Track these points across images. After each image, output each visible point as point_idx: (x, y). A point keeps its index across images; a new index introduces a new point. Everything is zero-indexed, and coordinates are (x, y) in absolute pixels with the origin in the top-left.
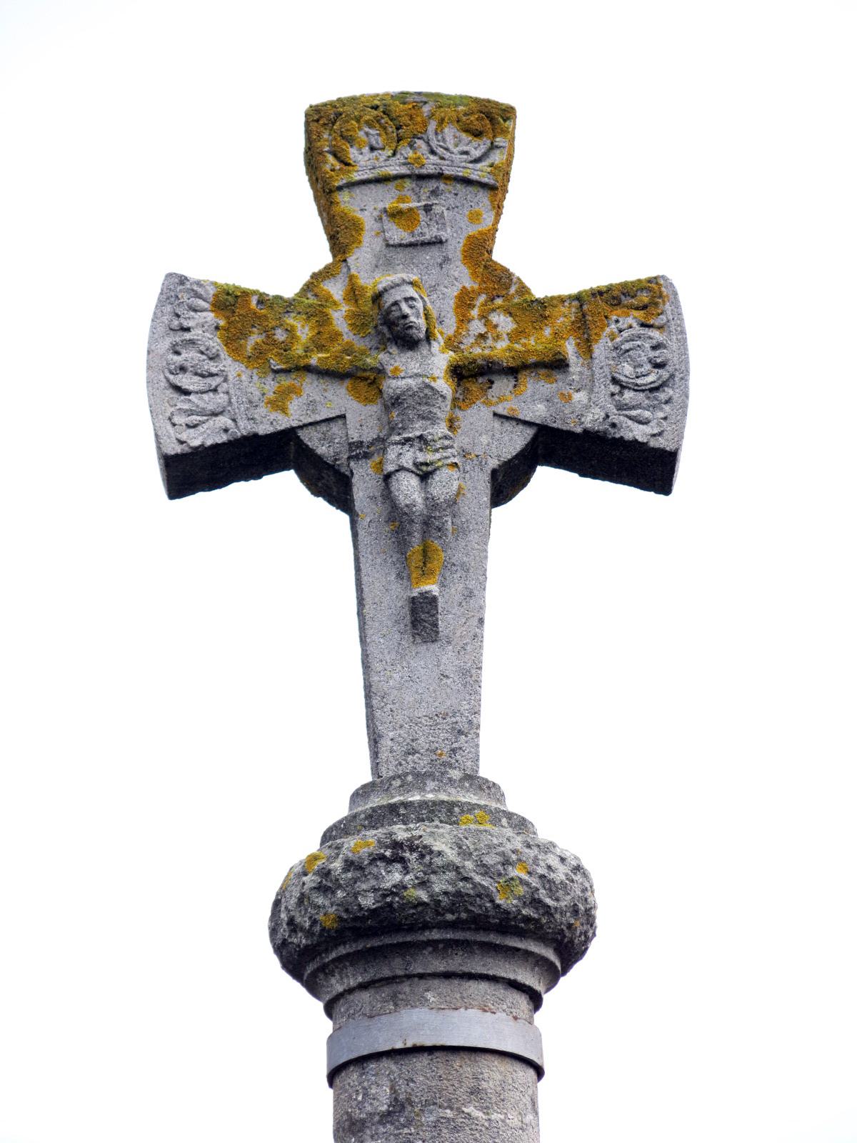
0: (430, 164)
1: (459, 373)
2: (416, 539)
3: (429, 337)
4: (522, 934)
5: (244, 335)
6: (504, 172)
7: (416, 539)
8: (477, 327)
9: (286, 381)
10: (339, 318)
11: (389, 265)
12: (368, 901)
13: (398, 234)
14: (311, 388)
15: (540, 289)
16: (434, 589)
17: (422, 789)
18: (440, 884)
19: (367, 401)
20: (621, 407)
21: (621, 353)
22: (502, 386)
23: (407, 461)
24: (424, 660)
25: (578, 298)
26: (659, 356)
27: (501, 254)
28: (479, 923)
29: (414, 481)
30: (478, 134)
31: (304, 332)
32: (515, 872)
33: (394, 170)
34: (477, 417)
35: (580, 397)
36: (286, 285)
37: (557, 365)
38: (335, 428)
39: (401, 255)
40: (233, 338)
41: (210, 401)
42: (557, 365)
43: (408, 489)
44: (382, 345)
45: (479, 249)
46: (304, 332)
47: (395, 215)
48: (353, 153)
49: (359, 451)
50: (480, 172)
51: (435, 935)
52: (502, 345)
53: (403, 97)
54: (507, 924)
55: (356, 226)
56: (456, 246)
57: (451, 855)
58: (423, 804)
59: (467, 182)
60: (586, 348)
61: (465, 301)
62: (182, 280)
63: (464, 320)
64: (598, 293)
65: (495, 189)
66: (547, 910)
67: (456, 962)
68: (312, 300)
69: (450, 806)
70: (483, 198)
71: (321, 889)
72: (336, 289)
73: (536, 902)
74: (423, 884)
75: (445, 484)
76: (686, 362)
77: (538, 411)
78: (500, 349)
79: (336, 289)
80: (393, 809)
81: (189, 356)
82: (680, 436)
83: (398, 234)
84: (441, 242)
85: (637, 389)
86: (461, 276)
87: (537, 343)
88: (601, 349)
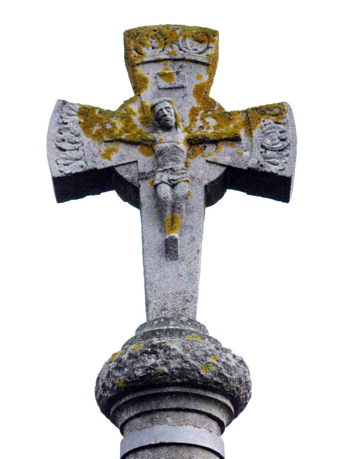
0: (179, 55)
2: (168, 214)
3: (176, 125)
4: (214, 391)
5: (92, 126)
7: (168, 214)
8: (199, 123)
9: (111, 146)
10: (136, 119)
11: (159, 96)
12: (139, 373)
13: (163, 83)
14: (122, 149)
15: (228, 108)
16: (176, 235)
18: (174, 364)
19: (148, 155)
20: (265, 158)
21: (265, 134)
22: (210, 148)
23: (165, 178)
25: (246, 112)
28: (193, 384)
29: (168, 188)
30: (201, 42)
32: (210, 360)
33: (163, 56)
35: (246, 154)
36: (113, 105)
37: (236, 139)
38: (133, 167)
39: (166, 92)
40: (86, 127)
41: (75, 154)
43: (165, 191)
44: (155, 131)
46: (120, 125)
47: (162, 75)
48: (144, 50)
49: (144, 177)
50: (201, 58)
51: (172, 389)
53: (168, 26)
55: (145, 80)
56: (190, 89)
57: (180, 351)
58: (168, 330)
59: (196, 62)
60: (249, 132)
61: (194, 112)
62: (64, 103)
63: (193, 120)
66: (226, 379)
67: (182, 403)
68: (124, 112)
69: (182, 330)
70: (203, 69)
71: (117, 368)
73: (221, 375)
74: (166, 364)
75: (182, 189)
77: (227, 160)
78: (210, 132)
79: (135, 107)
81: (66, 135)
82: (293, 170)
83: (163, 83)
84: (183, 87)
85: (273, 150)
86: (193, 102)
88: (256, 133)
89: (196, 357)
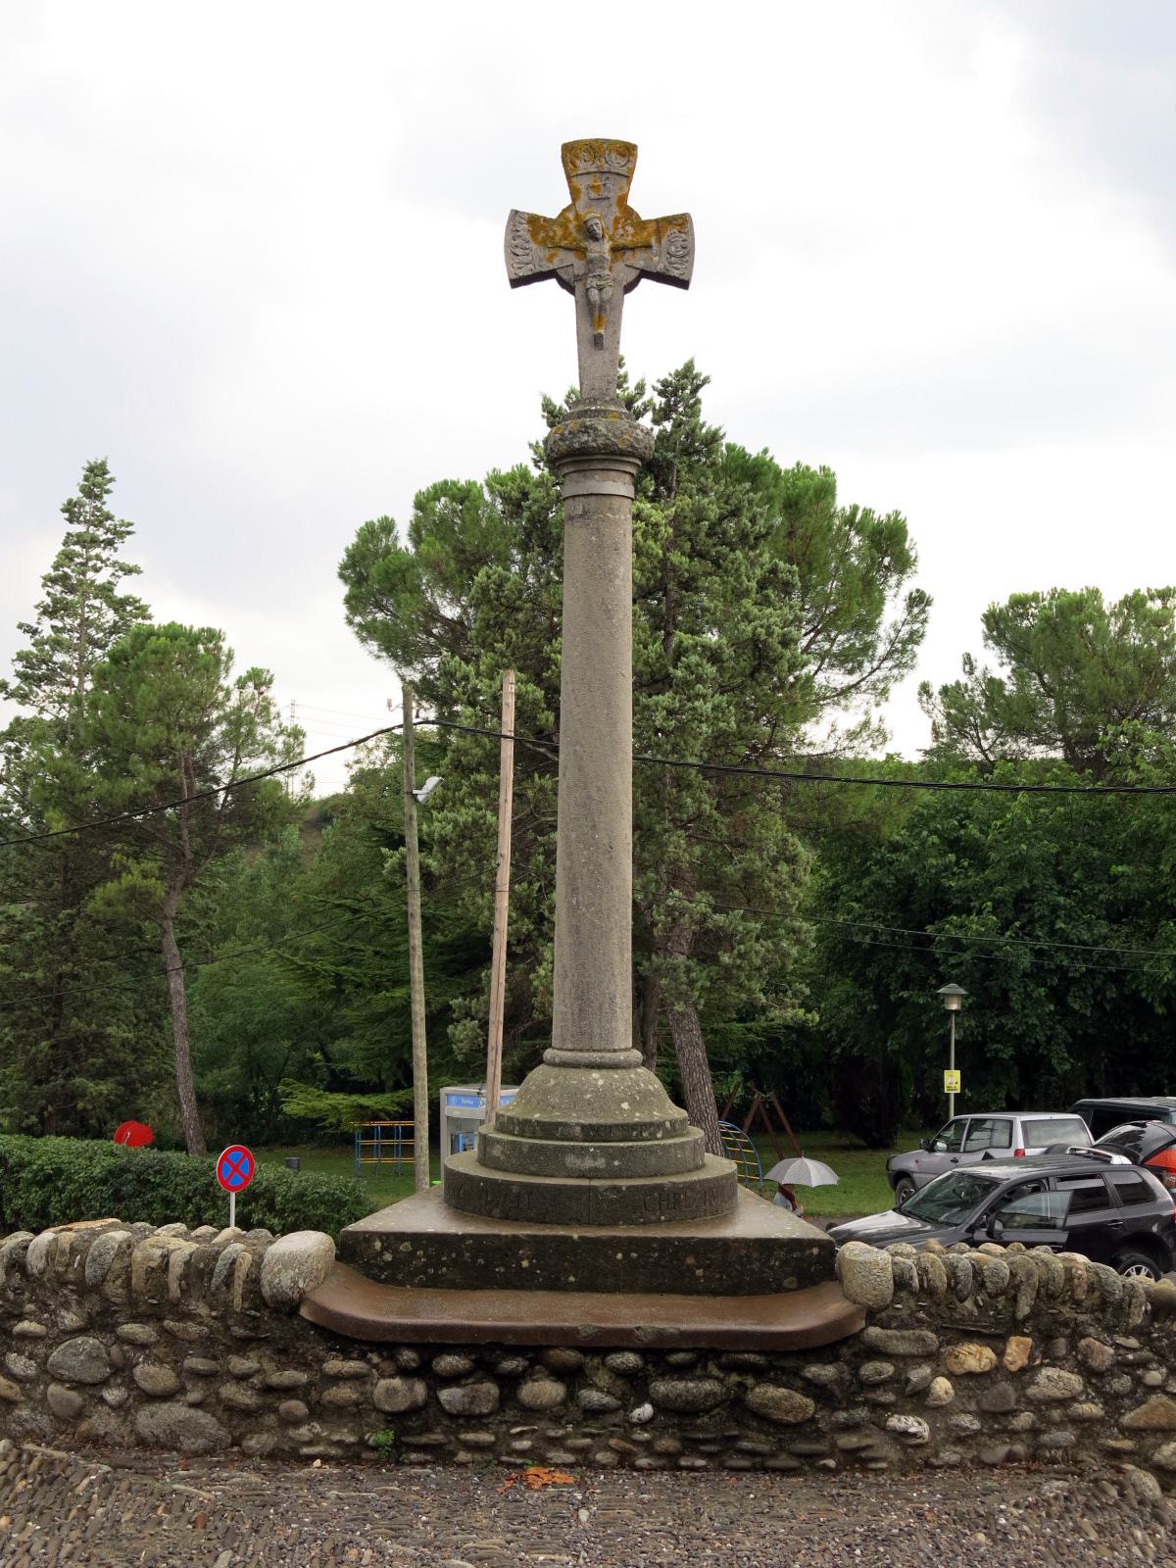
0: (606, 167)
1: (614, 250)
2: (597, 313)
3: (603, 236)
4: (627, 456)
5: (538, 234)
6: (632, 171)
7: (597, 313)
8: (621, 232)
9: (553, 251)
10: (572, 226)
11: (590, 206)
12: (577, 446)
13: (593, 195)
14: (561, 254)
15: (644, 217)
16: (602, 331)
17: (596, 405)
18: (600, 441)
19: (581, 259)
20: (670, 263)
21: (671, 242)
22: (629, 254)
23: (594, 284)
24: (599, 356)
25: (657, 221)
26: (685, 244)
27: (630, 203)
28: (613, 453)
29: (596, 292)
30: (623, 156)
31: (559, 232)
32: (625, 437)
33: (593, 170)
34: (620, 266)
35: (656, 259)
36: (553, 214)
37: (648, 247)
38: (570, 269)
39: (594, 203)
40: (534, 234)
41: (525, 259)
42: (648, 247)
43: (594, 294)
44: (586, 240)
45: (623, 200)
47: (593, 187)
48: (578, 163)
49: (578, 278)
50: (624, 171)
51: (598, 457)
52: (630, 238)
53: (597, 140)
54: (622, 453)
56: (614, 201)
57: (604, 431)
58: (596, 410)
59: (618, 174)
60: (659, 241)
61: (617, 221)
62: (516, 212)
63: (616, 228)
64: (664, 219)
65: (628, 178)
66: (636, 449)
67: (605, 465)
68: (562, 220)
69: (605, 411)
70: (624, 180)
71: (561, 439)
72: (571, 216)
73: (632, 446)
74: (595, 441)
75: (608, 292)
76: (693, 247)
77: (641, 264)
78: (628, 240)
79: (571, 216)
80: (586, 411)
81: (518, 241)
82: (690, 274)
83: (593, 195)
84: (608, 198)
86: (616, 211)
87: (640, 239)
88: (664, 241)
89: (615, 436)
